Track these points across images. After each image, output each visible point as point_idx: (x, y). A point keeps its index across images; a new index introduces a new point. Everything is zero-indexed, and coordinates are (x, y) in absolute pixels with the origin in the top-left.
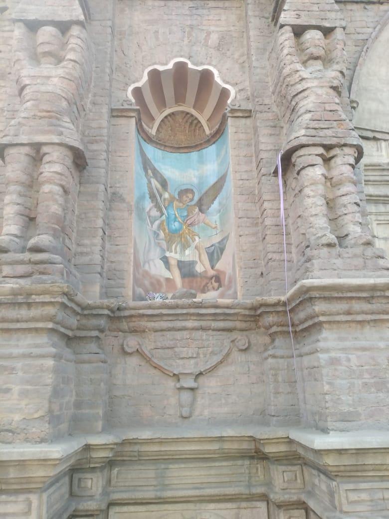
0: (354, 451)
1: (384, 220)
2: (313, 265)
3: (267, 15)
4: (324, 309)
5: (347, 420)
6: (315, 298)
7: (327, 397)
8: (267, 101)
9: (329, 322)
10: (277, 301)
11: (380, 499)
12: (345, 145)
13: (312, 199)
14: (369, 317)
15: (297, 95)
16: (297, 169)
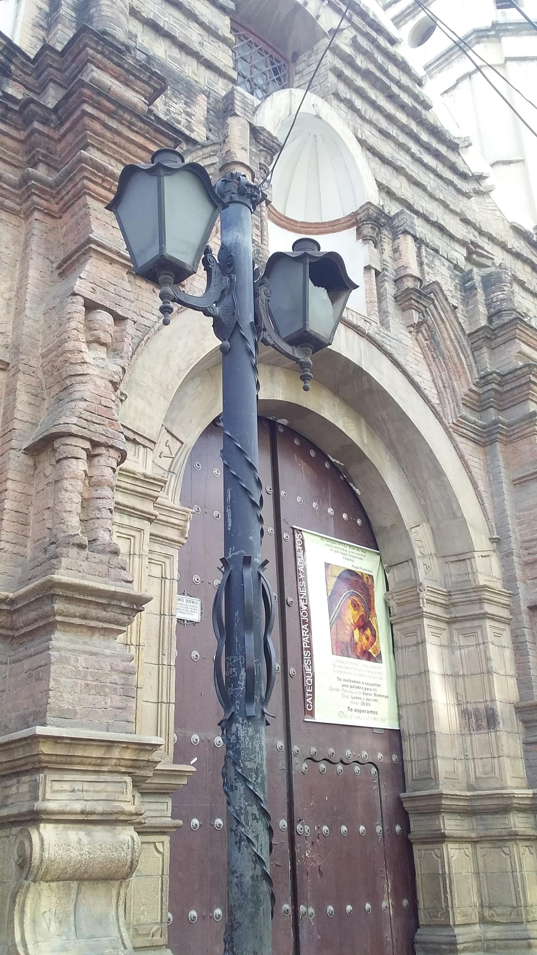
0: (68, 741)
1: (125, 534)
2: (61, 562)
3: (52, 258)
4: (63, 609)
5: (65, 716)
6: (58, 595)
7: (51, 693)
8: (33, 362)
9: (63, 623)
10: (3, 597)
11: (79, 790)
12: (112, 447)
13: (69, 494)
14: (101, 625)
15: (74, 375)
16: (58, 456)
